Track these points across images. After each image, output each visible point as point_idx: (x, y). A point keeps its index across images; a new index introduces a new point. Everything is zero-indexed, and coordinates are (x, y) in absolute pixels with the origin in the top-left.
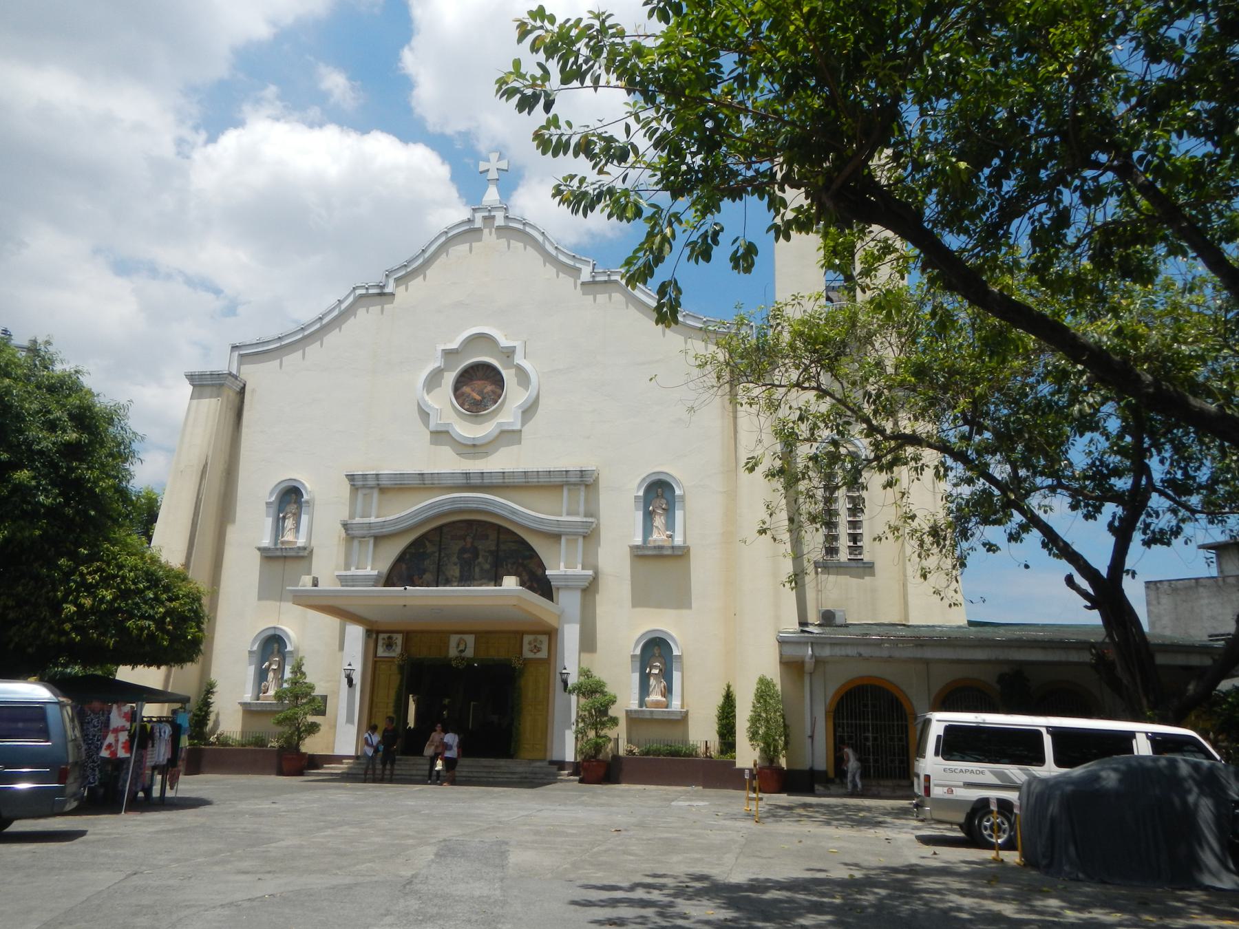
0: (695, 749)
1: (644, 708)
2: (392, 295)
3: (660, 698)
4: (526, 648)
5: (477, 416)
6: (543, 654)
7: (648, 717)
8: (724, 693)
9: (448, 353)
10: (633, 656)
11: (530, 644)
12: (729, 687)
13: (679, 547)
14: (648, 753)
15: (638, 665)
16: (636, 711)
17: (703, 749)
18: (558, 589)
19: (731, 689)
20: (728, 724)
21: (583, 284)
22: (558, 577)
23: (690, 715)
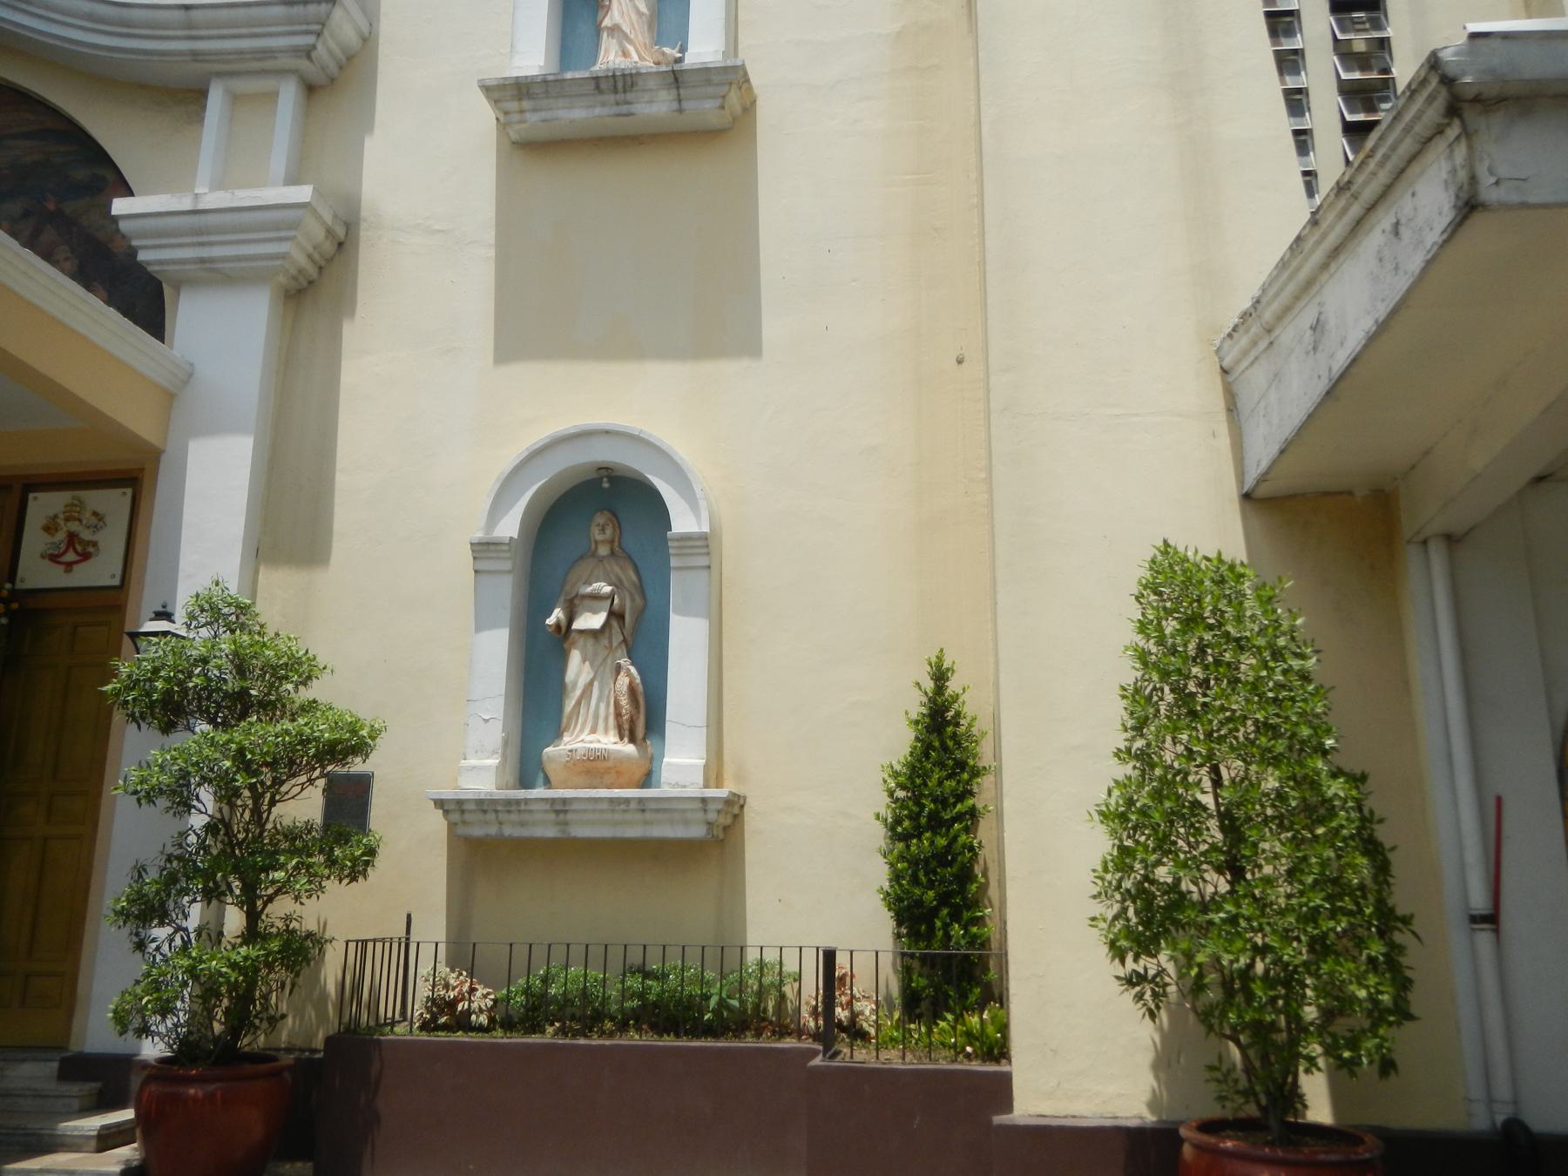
0: (773, 983)
1: (539, 792)
3: (608, 741)
4: (34, 541)
6: (101, 572)
7: (547, 831)
8: (916, 706)
10: (483, 549)
11: (50, 528)
12: (940, 676)
13: (706, 74)
14: (535, 1012)
15: (505, 590)
16: (484, 806)
17: (811, 987)
18: (177, 287)
19: (953, 686)
20: (942, 858)
22: (166, 227)
23: (753, 820)
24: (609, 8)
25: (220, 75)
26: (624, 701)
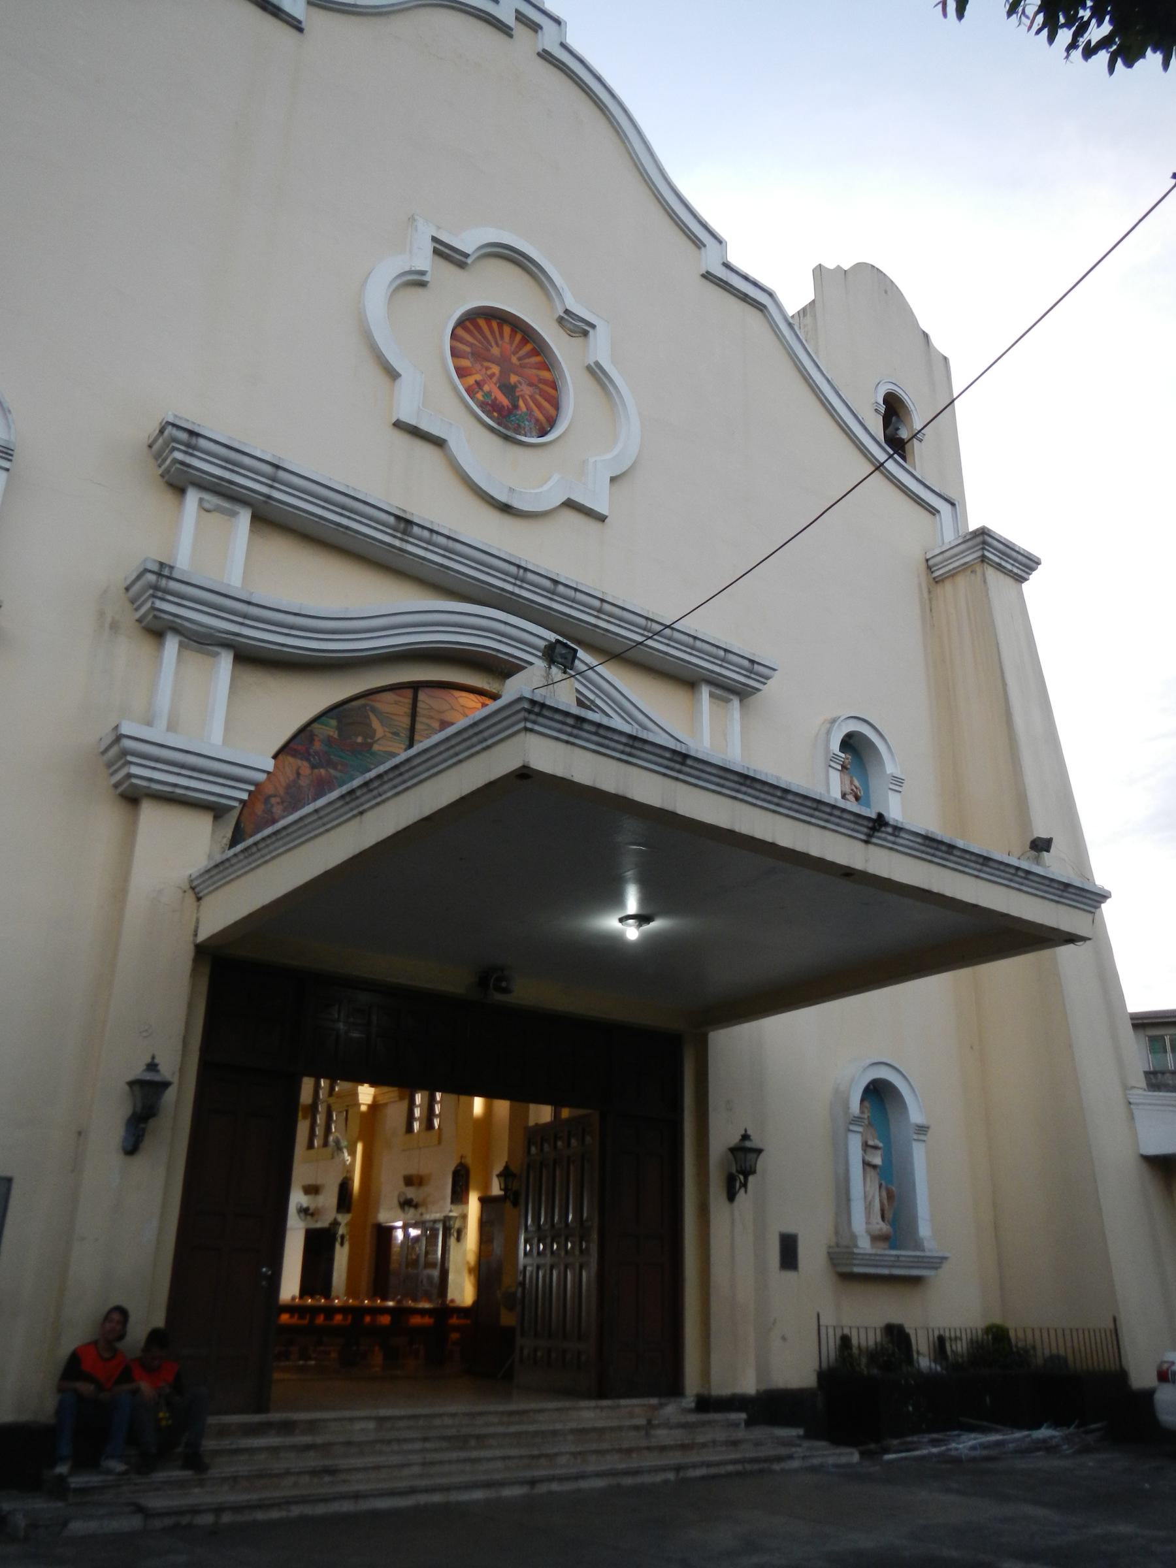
5: (506, 438)
9: (445, 252)
21: (708, 276)
26: (885, 1202)
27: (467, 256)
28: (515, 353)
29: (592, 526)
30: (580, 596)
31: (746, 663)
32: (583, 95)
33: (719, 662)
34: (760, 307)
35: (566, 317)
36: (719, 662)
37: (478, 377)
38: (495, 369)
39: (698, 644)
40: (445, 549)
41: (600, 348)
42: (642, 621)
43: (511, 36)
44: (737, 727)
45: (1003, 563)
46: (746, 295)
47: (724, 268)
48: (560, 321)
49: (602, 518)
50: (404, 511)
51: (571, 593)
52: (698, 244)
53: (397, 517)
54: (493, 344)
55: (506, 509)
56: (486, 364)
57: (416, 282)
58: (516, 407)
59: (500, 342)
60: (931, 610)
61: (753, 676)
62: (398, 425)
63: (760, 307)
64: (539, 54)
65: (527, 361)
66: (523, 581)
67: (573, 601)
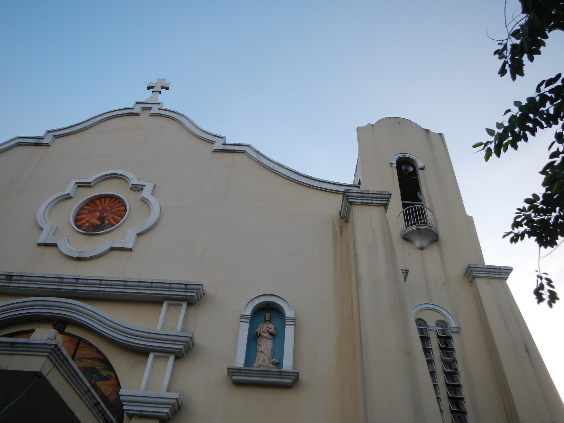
2: (47, 145)
5: (90, 235)
9: (81, 185)
21: (215, 151)
24: (261, 346)
25: (154, 351)
27: (90, 183)
28: (108, 206)
29: (126, 254)
30: (89, 281)
31: (183, 286)
32: (168, 119)
33: (168, 289)
34: (243, 152)
35: (132, 187)
36: (168, 289)
37: (88, 219)
38: (98, 214)
39: (141, 284)
40: (27, 281)
41: (146, 193)
42: (123, 283)
43: (139, 115)
44: (182, 315)
45: (364, 201)
46: (234, 150)
47: (223, 146)
48: (131, 189)
49: (130, 250)
50: (11, 272)
51: (86, 281)
52: (213, 142)
53: (7, 276)
54: (99, 205)
55: (79, 259)
56: (93, 214)
57: (68, 197)
58: (103, 223)
59: (103, 204)
60: (341, 235)
61: (188, 291)
62: (40, 245)
63: (243, 152)
64: (150, 115)
65: (115, 206)
66: (62, 283)
67: (87, 284)
